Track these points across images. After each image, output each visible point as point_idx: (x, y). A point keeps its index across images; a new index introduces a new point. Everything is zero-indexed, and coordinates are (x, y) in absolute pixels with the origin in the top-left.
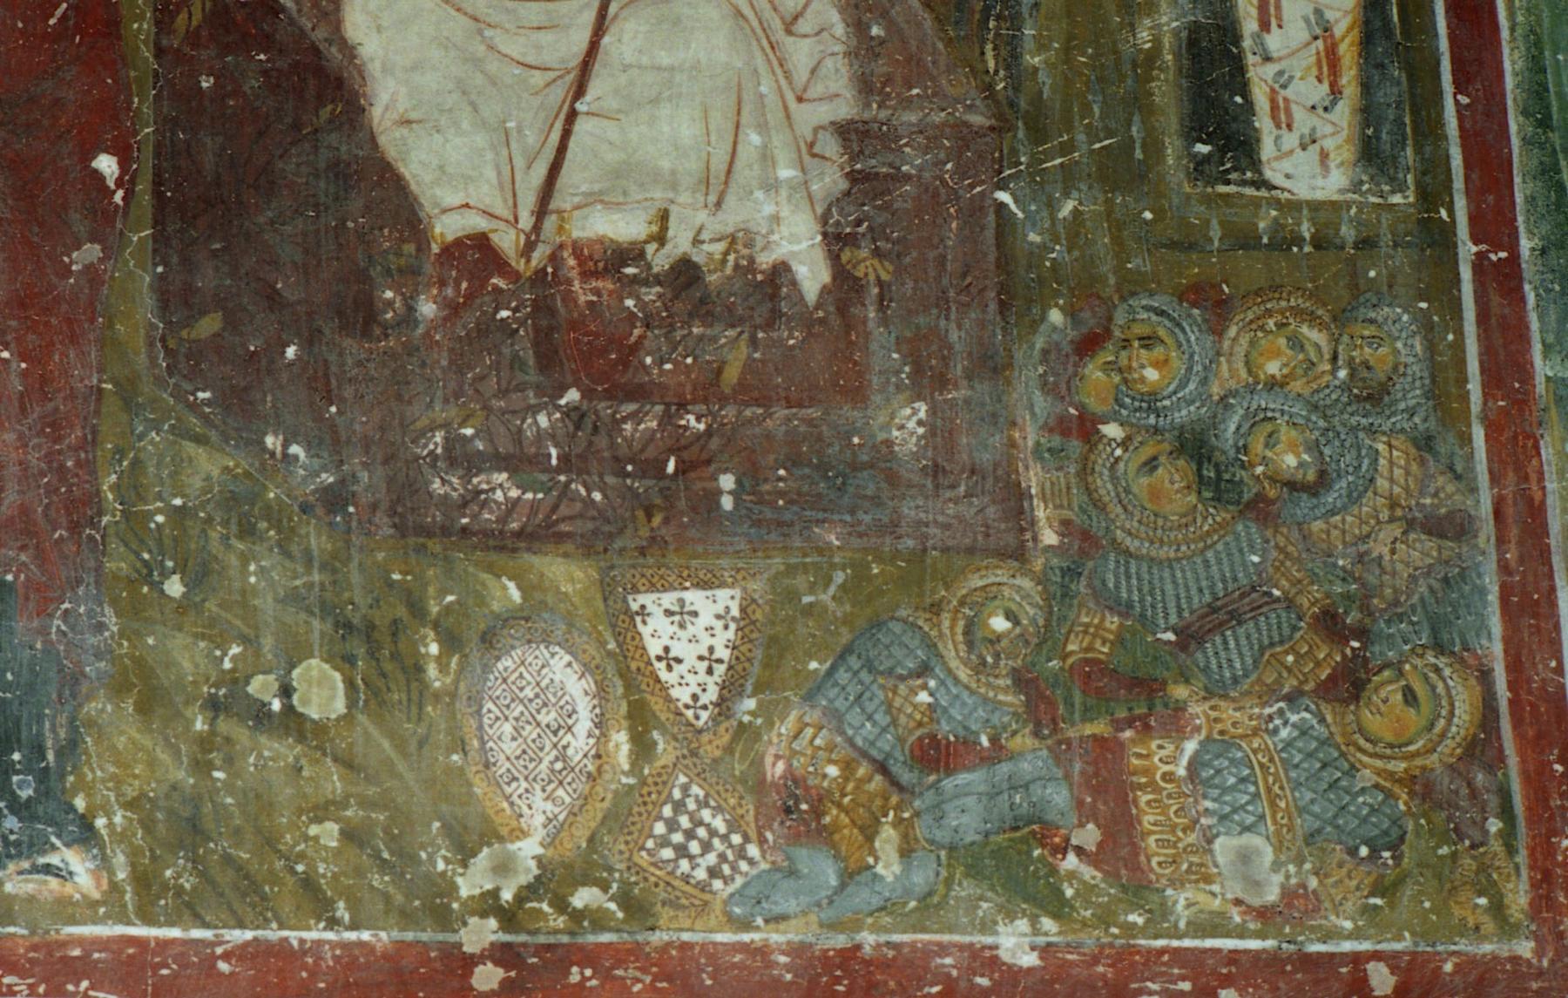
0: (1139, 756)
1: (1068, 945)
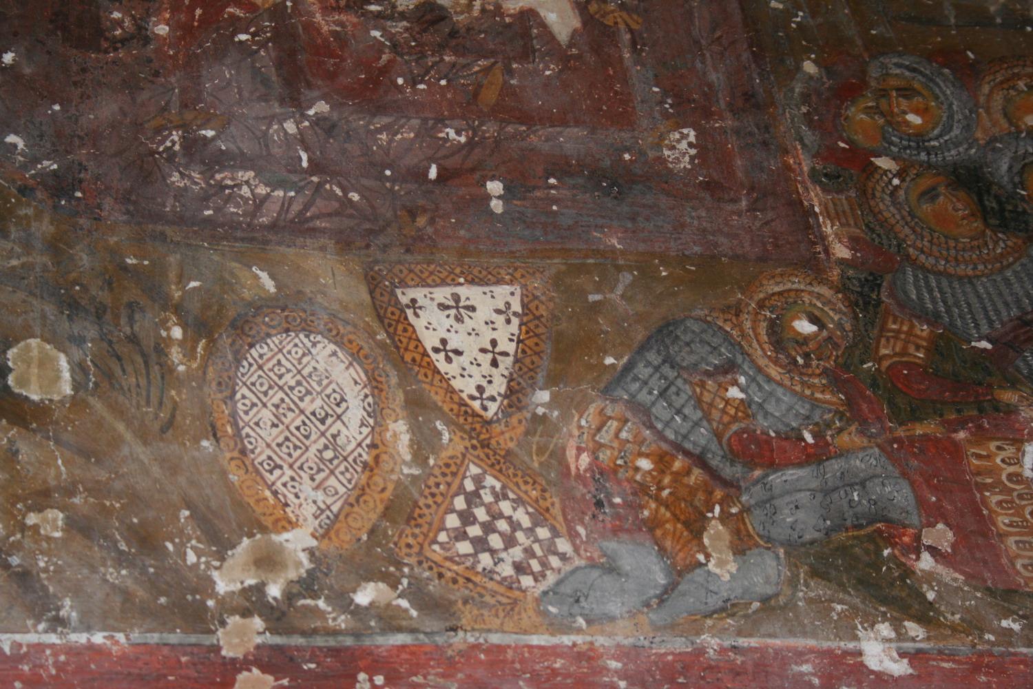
0: (979, 456)
1: (940, 652)
